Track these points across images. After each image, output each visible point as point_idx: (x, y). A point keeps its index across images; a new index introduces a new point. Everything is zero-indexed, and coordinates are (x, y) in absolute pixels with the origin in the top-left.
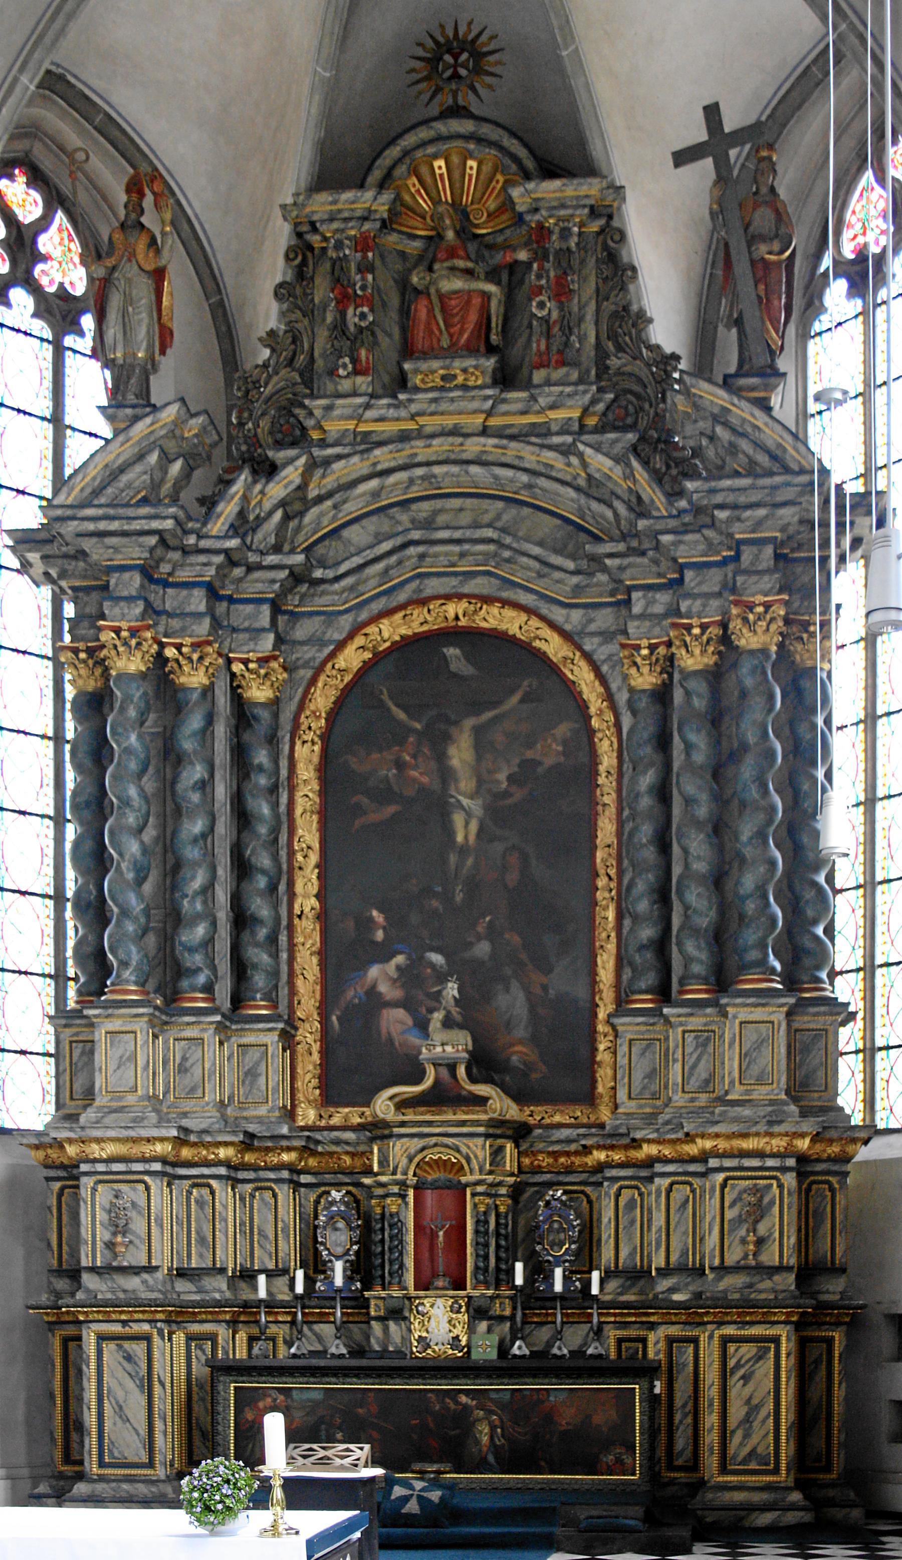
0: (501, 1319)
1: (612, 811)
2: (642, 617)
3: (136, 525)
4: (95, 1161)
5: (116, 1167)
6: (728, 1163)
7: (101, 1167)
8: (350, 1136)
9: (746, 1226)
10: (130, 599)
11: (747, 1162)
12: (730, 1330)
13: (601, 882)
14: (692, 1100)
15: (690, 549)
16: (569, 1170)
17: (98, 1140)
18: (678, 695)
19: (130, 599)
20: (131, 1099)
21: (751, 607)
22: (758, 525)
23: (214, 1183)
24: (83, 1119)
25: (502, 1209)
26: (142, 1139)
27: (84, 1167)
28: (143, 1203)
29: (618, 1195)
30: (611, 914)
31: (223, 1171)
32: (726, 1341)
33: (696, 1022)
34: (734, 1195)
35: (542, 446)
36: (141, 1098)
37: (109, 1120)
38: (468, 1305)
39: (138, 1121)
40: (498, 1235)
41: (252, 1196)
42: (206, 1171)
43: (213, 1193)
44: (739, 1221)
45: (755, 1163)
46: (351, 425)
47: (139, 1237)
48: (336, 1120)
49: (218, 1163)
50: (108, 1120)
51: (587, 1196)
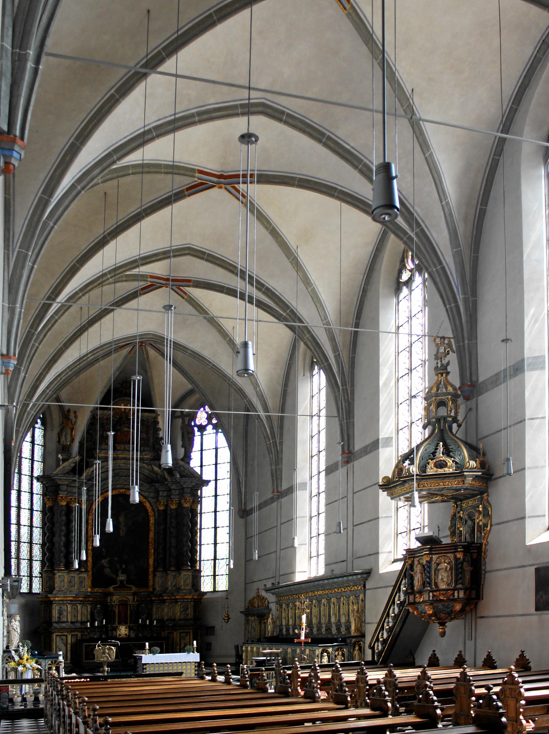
1: (153, 531)
2: (161, 496)
3: (69, 478)
8: (98, 594)
10: (64, 491)
12: (181, 631)
13: (150, 545)
15: (173, 487)
17: (58, 597)
18: (169, 512)
19: (64, 491)
20: (63, 589)
21: (186, 500)
22: (188, 485)
30: (152, 551)
32: (180, 633)
33: (173, 574)
35: (143, 463)
37: (59, 593)
46: (104, 455)
48: (95, 591)
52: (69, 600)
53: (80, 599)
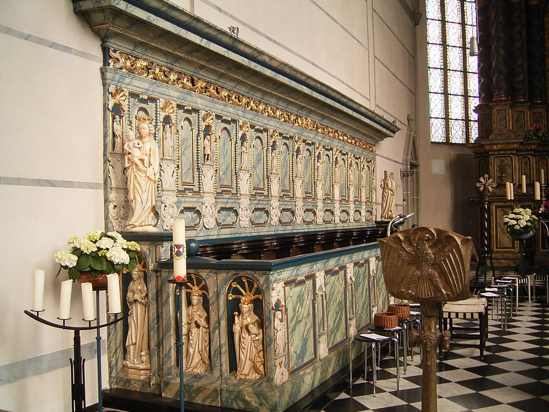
4: (495, 151)
7: (496, 153)
17: (496, 144)
20: (505, 131)
24: (490, 138)
27: (491, 153)
28: (510, 163)
37: (499, 138)
41: (539, 161)
52: (513, 149)
53: (533, 147)
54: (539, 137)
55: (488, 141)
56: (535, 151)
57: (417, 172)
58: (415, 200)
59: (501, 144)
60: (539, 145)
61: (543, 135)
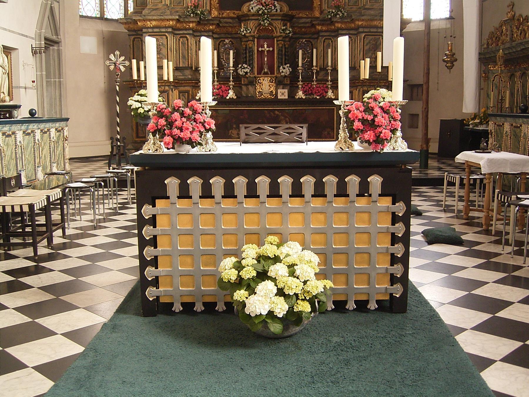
0: (286, 85)
4: (148, 28)
5: (156, 30)
6: (366, 30)
7: (150, 30)
9: (371, 52)
11: (372, 30)
14: (351, 8)
16: (305, 34)
17: (150, 20)
20: (160, 6)
23: (187, 36)
24: (143, 13)
25: (287, 46)
26: (165, 19)
27: (144, 30)
29: (324, 42)
31: (191, 32)
34: (368, 41)
36: (164, 5)
38: (275, 80)
39: (163, 13)
40: (285, 55)
42: (185, 32)
43: (188, 40)
44: (369, 50)
45: (375, 30)
47: (164, 56)
49: (189, 29)
50: (152, 13)
51: (311, 42)
53: (191, 25)
54: (197, 14)
55: (141, 16)
56: (174, 29)
57: (59, 50)
58: (57, 83)
59: (155, 20)
60: (199, 23)
61: (202, 13)
